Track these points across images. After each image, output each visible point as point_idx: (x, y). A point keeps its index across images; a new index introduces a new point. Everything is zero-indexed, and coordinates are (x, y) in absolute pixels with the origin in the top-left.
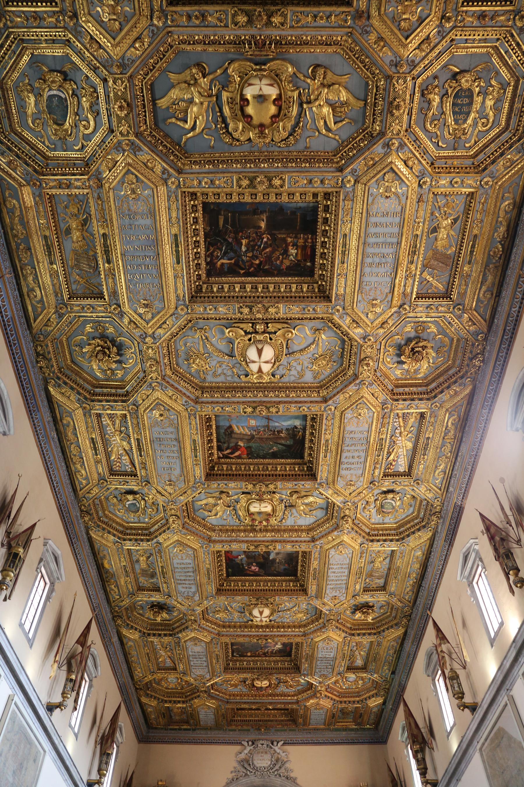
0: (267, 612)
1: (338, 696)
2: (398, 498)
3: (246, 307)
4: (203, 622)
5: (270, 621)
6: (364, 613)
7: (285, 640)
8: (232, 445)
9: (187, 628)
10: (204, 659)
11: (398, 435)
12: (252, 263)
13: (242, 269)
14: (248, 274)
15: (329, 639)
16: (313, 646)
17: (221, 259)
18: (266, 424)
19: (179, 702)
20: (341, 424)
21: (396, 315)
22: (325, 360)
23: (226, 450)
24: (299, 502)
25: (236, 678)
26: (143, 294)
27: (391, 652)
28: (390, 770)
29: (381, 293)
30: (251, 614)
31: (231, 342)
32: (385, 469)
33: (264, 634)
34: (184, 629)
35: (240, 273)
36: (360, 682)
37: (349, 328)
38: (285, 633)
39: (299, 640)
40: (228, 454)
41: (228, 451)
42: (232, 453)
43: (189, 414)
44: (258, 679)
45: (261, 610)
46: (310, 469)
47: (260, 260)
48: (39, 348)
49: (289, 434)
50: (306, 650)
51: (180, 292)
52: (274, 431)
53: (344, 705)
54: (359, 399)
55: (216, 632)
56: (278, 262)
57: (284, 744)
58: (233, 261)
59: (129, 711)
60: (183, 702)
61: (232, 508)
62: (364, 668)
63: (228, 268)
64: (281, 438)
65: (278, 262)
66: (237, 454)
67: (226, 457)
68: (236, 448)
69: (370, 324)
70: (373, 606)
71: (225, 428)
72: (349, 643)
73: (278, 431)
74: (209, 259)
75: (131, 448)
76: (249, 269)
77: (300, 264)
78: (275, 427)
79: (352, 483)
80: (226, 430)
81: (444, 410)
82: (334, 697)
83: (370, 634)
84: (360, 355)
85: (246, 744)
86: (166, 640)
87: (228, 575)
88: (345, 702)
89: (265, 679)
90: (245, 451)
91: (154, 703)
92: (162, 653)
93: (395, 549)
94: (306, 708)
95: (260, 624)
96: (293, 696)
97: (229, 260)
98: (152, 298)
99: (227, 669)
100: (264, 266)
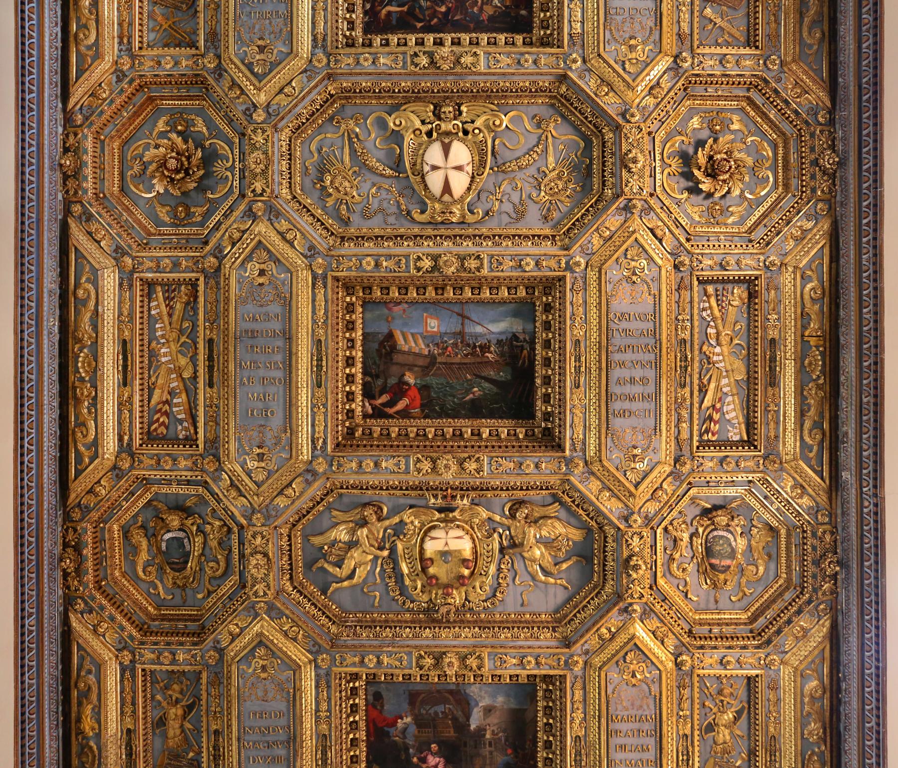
2: (739, 530)
3: (424, 53)
8: (392, 381)
11: (713, 342)
12: (435, 11)
13: (420, 21)
14: (428, 29)
17: (387, 5)
18: (458, 329)
20: (600, 297)
21: (672, 73)
22: (560, 178)
23: (381, 395)
24: (532, 531)
26: (260, 30)
29: (642, 28)
31: (397, 137)
32: (701, 435)
35: (415, 26)
37: (596, 95)
40: (384, 405)
41: (385, 398)
42: (391, 403)
43: (315, 278)
46: (548, 432)
47: (447, 6)
48: (71, 138)
49: (502, 354)
51: (320, 28)
52: (475, 347)
54: (629, 237)
56: (475, 9)
58: (405, 9)
61: (386, 553)
63: (398, 20)
64: (488, 363)
65: (475, 9)
66: (401, 405)
67: (378, 413)
68: (400, 389)
69: (630, 81)
71: (381, 337)
73: (480, 346)
74: (368, 6)
75: (196, 372)
76: (430, 21)
77: (510, 13)
78: (477, 336)
79: (637, 451)
80: (381, 344)
81: (790, 269)
84: (621, 150)
90: (418, 396)
93: (754, 672)
97: (399, 6)
98: (272, 36)
100: (453, 17)
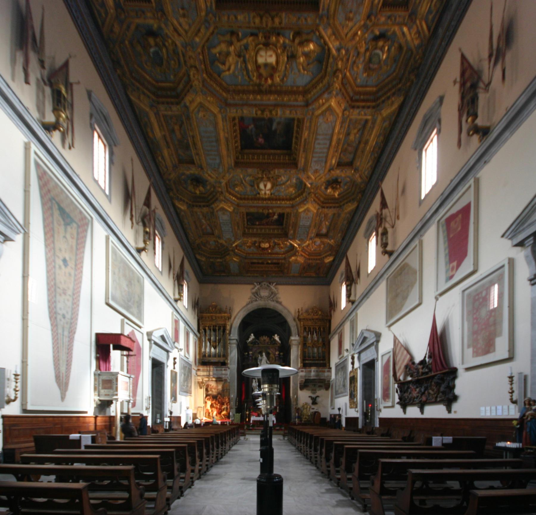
0: (269, 186)
1: (308, 255)
4: (227, 194)
5: (271, 194)
6: (333, 188)
7: (280, 211)
9: (217, 199)
10: (230, 226)
15: (308, 210)
16: (297, 215)
19: (218, 258)
25: (250, 240)
27: (345, 222)
28: (330, 298)
30: (258, 187)
33: (267, 205)
34: (215, 201)
36: (322, 246)
38: (281, 205)
39: (288, 210)
44: (263, 242)
45: (265, 183)
50: (293, 219)
53: (310, 261)
55: (236, 203)
57: (276, 284)
59: (187, 258)
60: (220, 258)
62: (326, 235)
70: (341, 182)
72: (320, 214)
82: (306, 256)
83: (334, 207)
85: (256, 284)
86: (205, 210)
87: (242, 149)
88: (312, 259)
89: (266, 242)
91: (203, 259)
92: (204, 221)
94: (290, 263)
95: (264, 196)
96: (283, 254)
99: (244, 234)
